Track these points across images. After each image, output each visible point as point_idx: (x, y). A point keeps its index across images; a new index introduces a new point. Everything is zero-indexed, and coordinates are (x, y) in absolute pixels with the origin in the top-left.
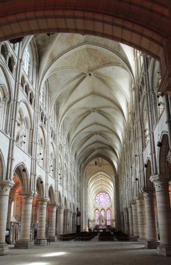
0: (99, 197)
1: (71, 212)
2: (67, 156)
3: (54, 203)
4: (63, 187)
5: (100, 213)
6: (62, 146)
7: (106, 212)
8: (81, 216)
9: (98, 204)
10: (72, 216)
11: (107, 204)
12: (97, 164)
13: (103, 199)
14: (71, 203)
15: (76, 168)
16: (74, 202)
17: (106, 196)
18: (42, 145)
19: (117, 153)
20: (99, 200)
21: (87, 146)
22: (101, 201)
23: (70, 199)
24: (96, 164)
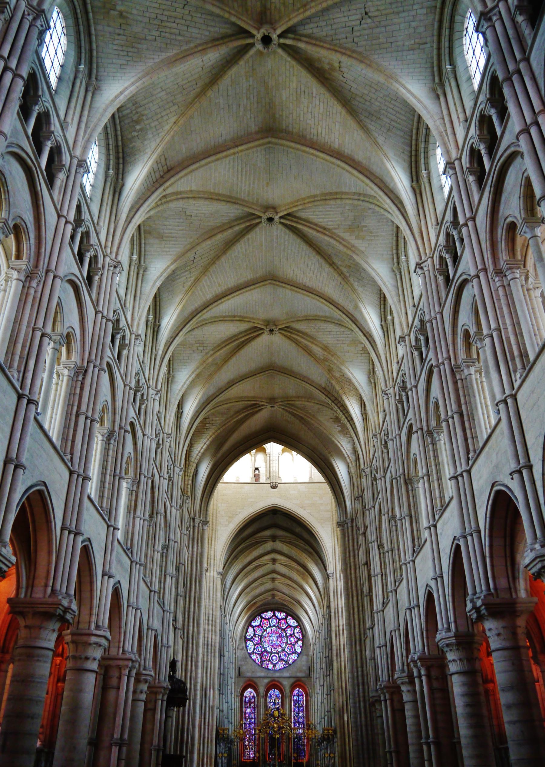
0: (259, 631)
1: (138, 674)
2: (142, 395)
3: (51, 600)
4: (108, 526)
5: (262, 700)
6: (128, 337)
7: (288, 700)
8: (184, 706)
9: (254, 661)
10: (143, 697)
11: (290, 662)
12: (261, 480)
13: (275, 639)
14: (145, 627)
15: (177, 470)
16: (156, 624)
17: (290, 626)
18: (18, 262)
19: (354, 416)
20: (260, 643)
21: (228, 383)
22: (269, 650)
23: (143, 604)
24: (257, 477)
